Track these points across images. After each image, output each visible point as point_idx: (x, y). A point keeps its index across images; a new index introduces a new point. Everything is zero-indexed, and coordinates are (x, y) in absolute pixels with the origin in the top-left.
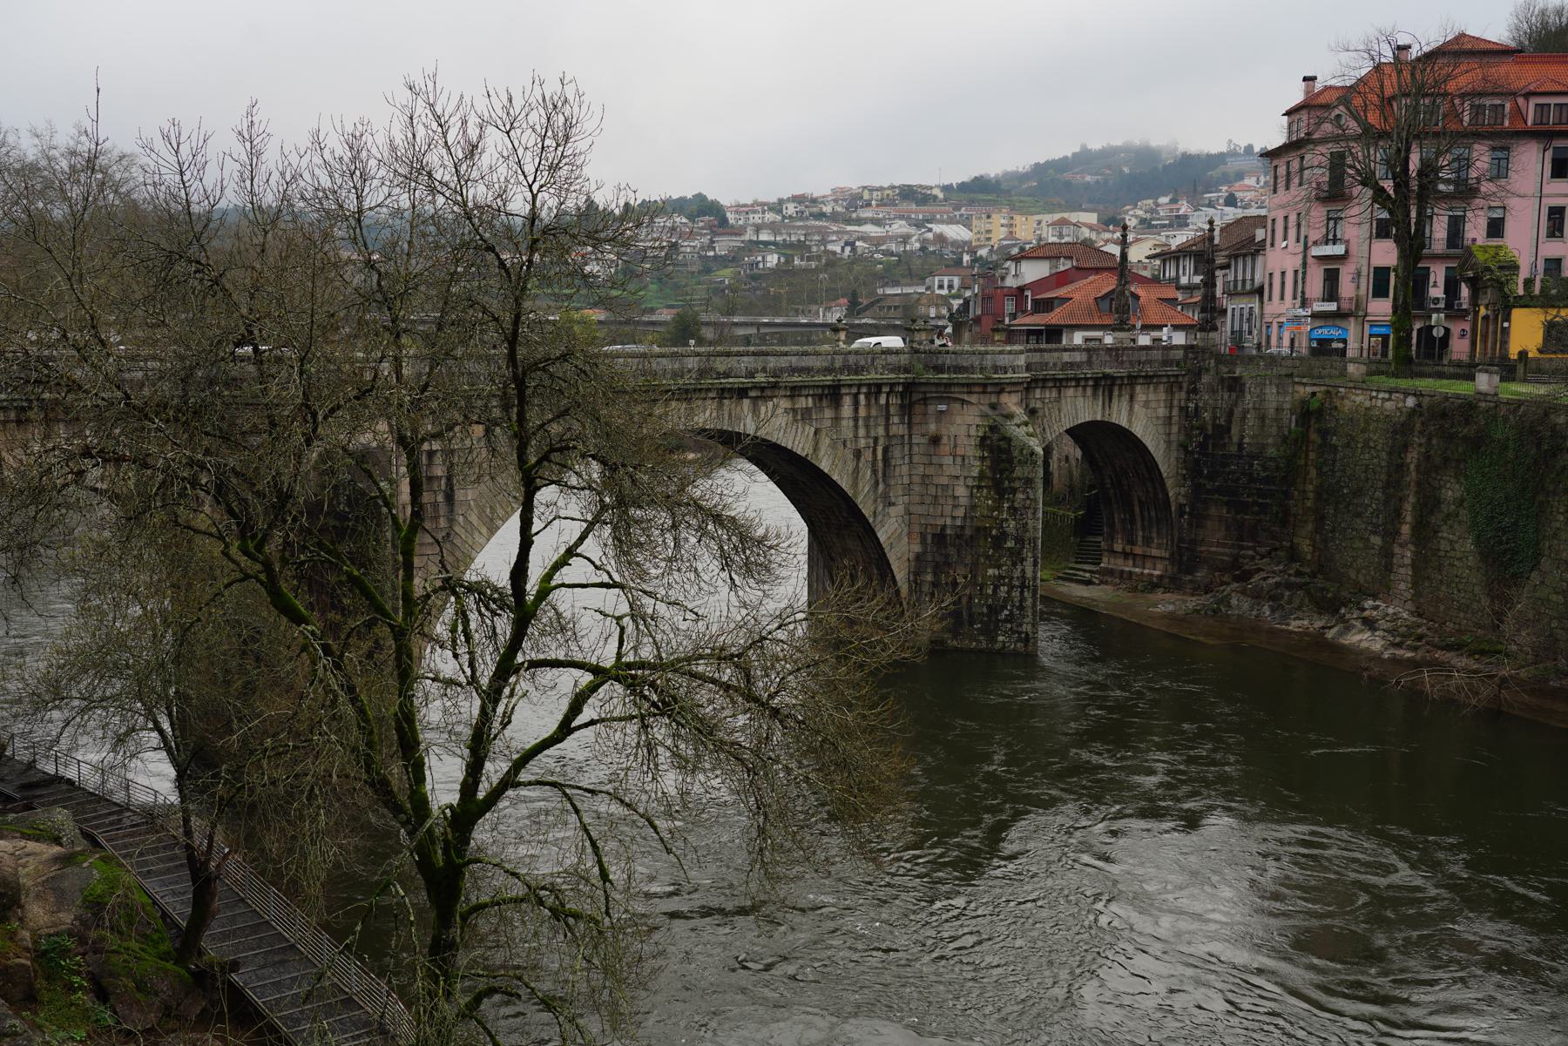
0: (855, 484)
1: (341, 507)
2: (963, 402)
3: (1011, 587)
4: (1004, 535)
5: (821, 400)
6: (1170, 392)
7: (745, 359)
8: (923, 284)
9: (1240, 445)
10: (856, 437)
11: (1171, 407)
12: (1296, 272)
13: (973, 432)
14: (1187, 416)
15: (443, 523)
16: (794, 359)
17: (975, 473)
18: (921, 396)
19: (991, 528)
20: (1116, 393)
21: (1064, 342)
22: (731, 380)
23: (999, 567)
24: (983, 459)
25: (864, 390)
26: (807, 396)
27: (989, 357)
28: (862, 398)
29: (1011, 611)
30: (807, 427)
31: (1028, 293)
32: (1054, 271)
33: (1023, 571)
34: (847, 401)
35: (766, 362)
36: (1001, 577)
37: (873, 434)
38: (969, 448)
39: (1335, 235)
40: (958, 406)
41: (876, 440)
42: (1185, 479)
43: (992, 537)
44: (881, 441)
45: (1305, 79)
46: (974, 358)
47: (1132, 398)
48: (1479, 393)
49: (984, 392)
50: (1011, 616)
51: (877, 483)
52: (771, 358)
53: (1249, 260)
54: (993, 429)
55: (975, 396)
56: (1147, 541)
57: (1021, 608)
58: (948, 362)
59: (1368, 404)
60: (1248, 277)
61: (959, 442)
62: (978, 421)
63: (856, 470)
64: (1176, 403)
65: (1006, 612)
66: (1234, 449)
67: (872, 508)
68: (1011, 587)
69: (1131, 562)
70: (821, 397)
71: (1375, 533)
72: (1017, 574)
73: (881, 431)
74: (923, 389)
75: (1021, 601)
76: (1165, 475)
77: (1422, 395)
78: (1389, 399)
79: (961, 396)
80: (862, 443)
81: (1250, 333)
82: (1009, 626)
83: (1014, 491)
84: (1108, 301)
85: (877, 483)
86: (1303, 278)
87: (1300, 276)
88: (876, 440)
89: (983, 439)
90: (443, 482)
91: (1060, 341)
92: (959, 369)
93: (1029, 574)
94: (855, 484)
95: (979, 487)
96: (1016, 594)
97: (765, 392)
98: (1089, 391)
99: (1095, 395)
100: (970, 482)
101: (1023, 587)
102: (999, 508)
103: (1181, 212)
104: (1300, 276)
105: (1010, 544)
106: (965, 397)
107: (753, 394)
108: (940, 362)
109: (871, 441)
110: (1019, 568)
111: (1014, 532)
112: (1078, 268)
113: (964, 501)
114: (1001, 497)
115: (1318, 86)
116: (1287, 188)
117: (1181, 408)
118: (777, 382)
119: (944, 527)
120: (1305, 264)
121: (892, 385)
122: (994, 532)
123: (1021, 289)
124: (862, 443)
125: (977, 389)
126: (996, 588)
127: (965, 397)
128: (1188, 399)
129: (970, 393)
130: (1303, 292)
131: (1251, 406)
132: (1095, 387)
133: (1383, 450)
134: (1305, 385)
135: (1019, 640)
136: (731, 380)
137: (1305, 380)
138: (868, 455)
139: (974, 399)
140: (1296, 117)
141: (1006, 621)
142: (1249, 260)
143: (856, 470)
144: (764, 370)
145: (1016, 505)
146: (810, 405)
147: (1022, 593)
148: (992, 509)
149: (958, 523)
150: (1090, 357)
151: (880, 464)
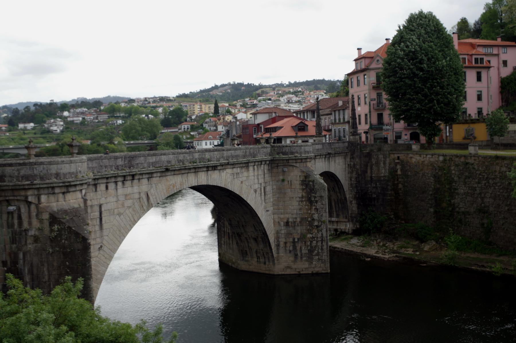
1: (63, 241)
2: (293, 166)
3: (317, 242)
4: (313, 220)
6: (345, 158)
7: (216, 153)
8: (178, 128)
9: (371, 177)
11: (346, 164)
12: (366, 115)
13: (298, 178)
14: (351, 168)
16: (233, 152)
17: (300, 195)
18: (276, 165)
19: (308, 218)
20: (331, 160)
21: (283, 142)
22: (212, 162)
23: (312, 234)
24: (303, 189)
27: (303, 148)
28: (256, 167)
29: (318, 251)
31: (262, 126)
32: (270, 118)
33: (322, 234)
34: (251, 168)
35: (223, 154)
36: (313, 238)
38: (297, 184)
39: (380, 101)
40: (291, 168)
41: (261, 184)
42: (352, 191)
43: (309, 221)
45: (358, 49)
46: (297, 148)
47: (335, 161)
48: (470, 154)
49: (301, 162)
50: (318, 254)
52: (225, 152)
53: (341, 112)
54: (306, 177)
56: (338, 216)
57: (322, 249)
58: (287, 150)
59: (423, 160)
60: (342, 117)
61: (292, 183)
62: (300, 174)
64: (347, 162)
65: (316, 252)
66: (369, 179)
68: (317, 242)
69: (336, 225)
71: (431, 207)
72: (319, 235)
74: (277, 162)
75: (322, 247)
76: (345, 190)
77: (446, 155)
78: (432, 158)
79: (292, 164)
81: (344, 137)
82: (317, 257)
83: (316, 202)
84: (297, 127)
86: (370, 117)
87: (368, 116)
89: (302, 181)
90: (98, 220)
91: (281, 143)
92: (292, 153)
93: (325, 235)
95: (302, 201)
96: (319, 244)
97: (224, 166)
98: (323, 159)
99: (325, 161)
101: (322, 241)
102: (310, 209)
103: (254, 103)
104: (368, 116)
105: (316, 223)
106: (295, 164)
108: (284, 151)
110: (320, 233)
111: (317, 218)
112: (279, 116)
114: (311, 205)
115: (363, 52)
116: (358, 85)
117: (348, 165)
118: (228, 162)
119: (288, 219)
120: (370, 112)
121: (266, 161)
122: (309, 219)
123: (258, 125)
125: (299, 161)
126: (311, 242)
128: (351, 161)
129: (296, 163)
130: (370, 122)
131: (374, 162)
132: (325, 158)
133: (431, 176)
134: (394, 154)
135: (322, 263)
136: (212, 162)
137: (394, 152)
138: (258, 191)
139: (298, 165)
140: (359, 61)
141: (316, 255)
142: (341, 112)
144: (223, 157)
145: (318, 207)
146: (239, 171)
147: (322, 243)
148: (307, 210)
149: (294, 216)
150: (323, 146)
151: (263, 194)
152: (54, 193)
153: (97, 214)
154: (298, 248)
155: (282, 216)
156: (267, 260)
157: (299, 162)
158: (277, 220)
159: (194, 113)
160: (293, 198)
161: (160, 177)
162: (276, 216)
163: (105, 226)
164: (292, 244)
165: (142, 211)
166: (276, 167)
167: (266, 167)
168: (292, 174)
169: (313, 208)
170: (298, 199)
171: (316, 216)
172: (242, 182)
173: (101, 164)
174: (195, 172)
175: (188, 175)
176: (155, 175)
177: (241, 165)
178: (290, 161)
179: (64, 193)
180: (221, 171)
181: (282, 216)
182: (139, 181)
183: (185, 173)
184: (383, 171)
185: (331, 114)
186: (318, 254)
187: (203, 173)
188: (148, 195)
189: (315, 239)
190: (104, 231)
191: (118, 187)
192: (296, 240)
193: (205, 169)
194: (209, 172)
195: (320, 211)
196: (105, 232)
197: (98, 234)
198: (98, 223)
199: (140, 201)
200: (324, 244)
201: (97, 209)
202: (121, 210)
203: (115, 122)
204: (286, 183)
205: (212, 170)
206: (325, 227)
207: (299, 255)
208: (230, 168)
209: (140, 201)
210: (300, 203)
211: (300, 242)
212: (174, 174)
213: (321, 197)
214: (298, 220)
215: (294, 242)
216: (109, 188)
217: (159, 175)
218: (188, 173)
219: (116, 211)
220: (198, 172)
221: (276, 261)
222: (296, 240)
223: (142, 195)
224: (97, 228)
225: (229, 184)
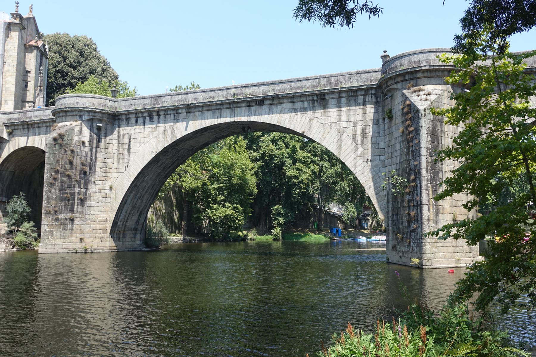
0: (340, 147)
5: (313, 103)
10: (340, 121)
15: (126, 160)
25: (343, 95)
26: (303, 101)
30: (304, 118)
37: (352, 119)
41: (355, 122)
44: (360, 123)
49: (404, 80)
51: (357, 148)
55: (400, 84)
63: (340, 140)
67: (353, 162)
70: (313, 101)
73: (360, 117)
79: (392, 87)
80: (344, 125)
85: (357, 148)
88: (355, 122)
90: (127, 145)
94: (340, 147)
106: (395, 86)
107: (267, 102)
109: (352, 124)
113: (398, 152)
124: (344, 125)
125: (399, 79)
127: (395, 86)
129: (396, 83)
143: (340, 140)
152: (60, 117)
153: (127, 141)
157: (401, 81)
160: (396, 138)
161: (187, 113)
163: (132, 150)
165: (165, 142)
169: (411, 150)
172: (311, 119)
173: (132, 103)
174: (230, 108)
175: (221, 112)
176: (180, 111)
177: (310, 98)
178: (390, 83)
179: (64, 116)
180: (273, 106)
182: (165, 117)
183: (217, 109)
187: (244, 108)
188: (173, 129)
190: (131, 154)
191: (146, 121)
193: (244, 105)
194: (253, 108)
195: (415, 154)
196: (132, 155)
197: (126, 155)
198: (127, 147)
199: (164, 133)
201: (127, 137)
202: (147, 139)
205: (256, 105)
208: (288, 102)
209: (164, 133)
212: (203, 110)
216: (139, 122)
217: (184, 111)
218: (221, 109)
219: (142, 140)
220: (234, 108)
223: (167, 128)
224: (126, 151)
225: (287, 120)
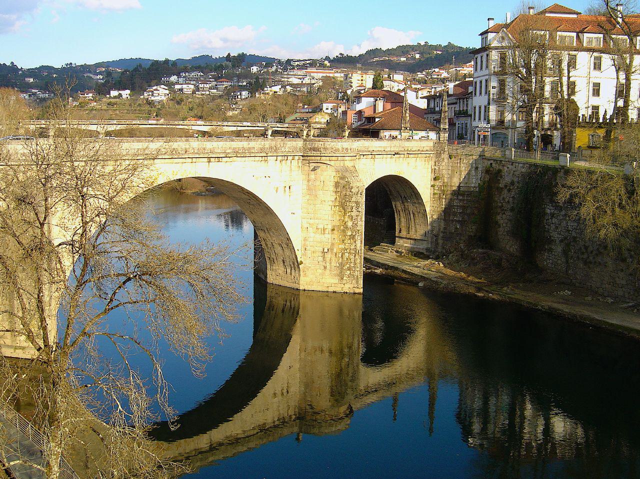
12: (485, 107)
50: (349, 269)
53: (465, 100)
57: (355, 264)
62: (334, 174)
81: (466, 135)
93: (358, 248)
100: (331, 203)
105: (349, 233)
106: (328, 162)
139: (332, 163)
142: (465, 100)
154: (328, 259)
155: (312, 221)
156: (293, 270)
158: (306, 226)
159: (351, 86)
162: (305, 221)
164: (321, 254)
166: (308, 165)
167: (295, 163)
168: (325, 173)
170: (331, 203)
171: (350, 224)
181: (312, 221)
184: (474, 181)
185: (456, 103)
186: (349, 269)
189: (348, 250)
192: (326, 250)
200: (357, 257)
203: (239, 94)
204: (318, 183)
206: (359, 238)
207: (328, 267)
210: (333, 207)
211: (330, 253)
213: (357, 203)
214: (330, 227)
215: (323, 252)
221: (301, 272)
222: (326, 250)
